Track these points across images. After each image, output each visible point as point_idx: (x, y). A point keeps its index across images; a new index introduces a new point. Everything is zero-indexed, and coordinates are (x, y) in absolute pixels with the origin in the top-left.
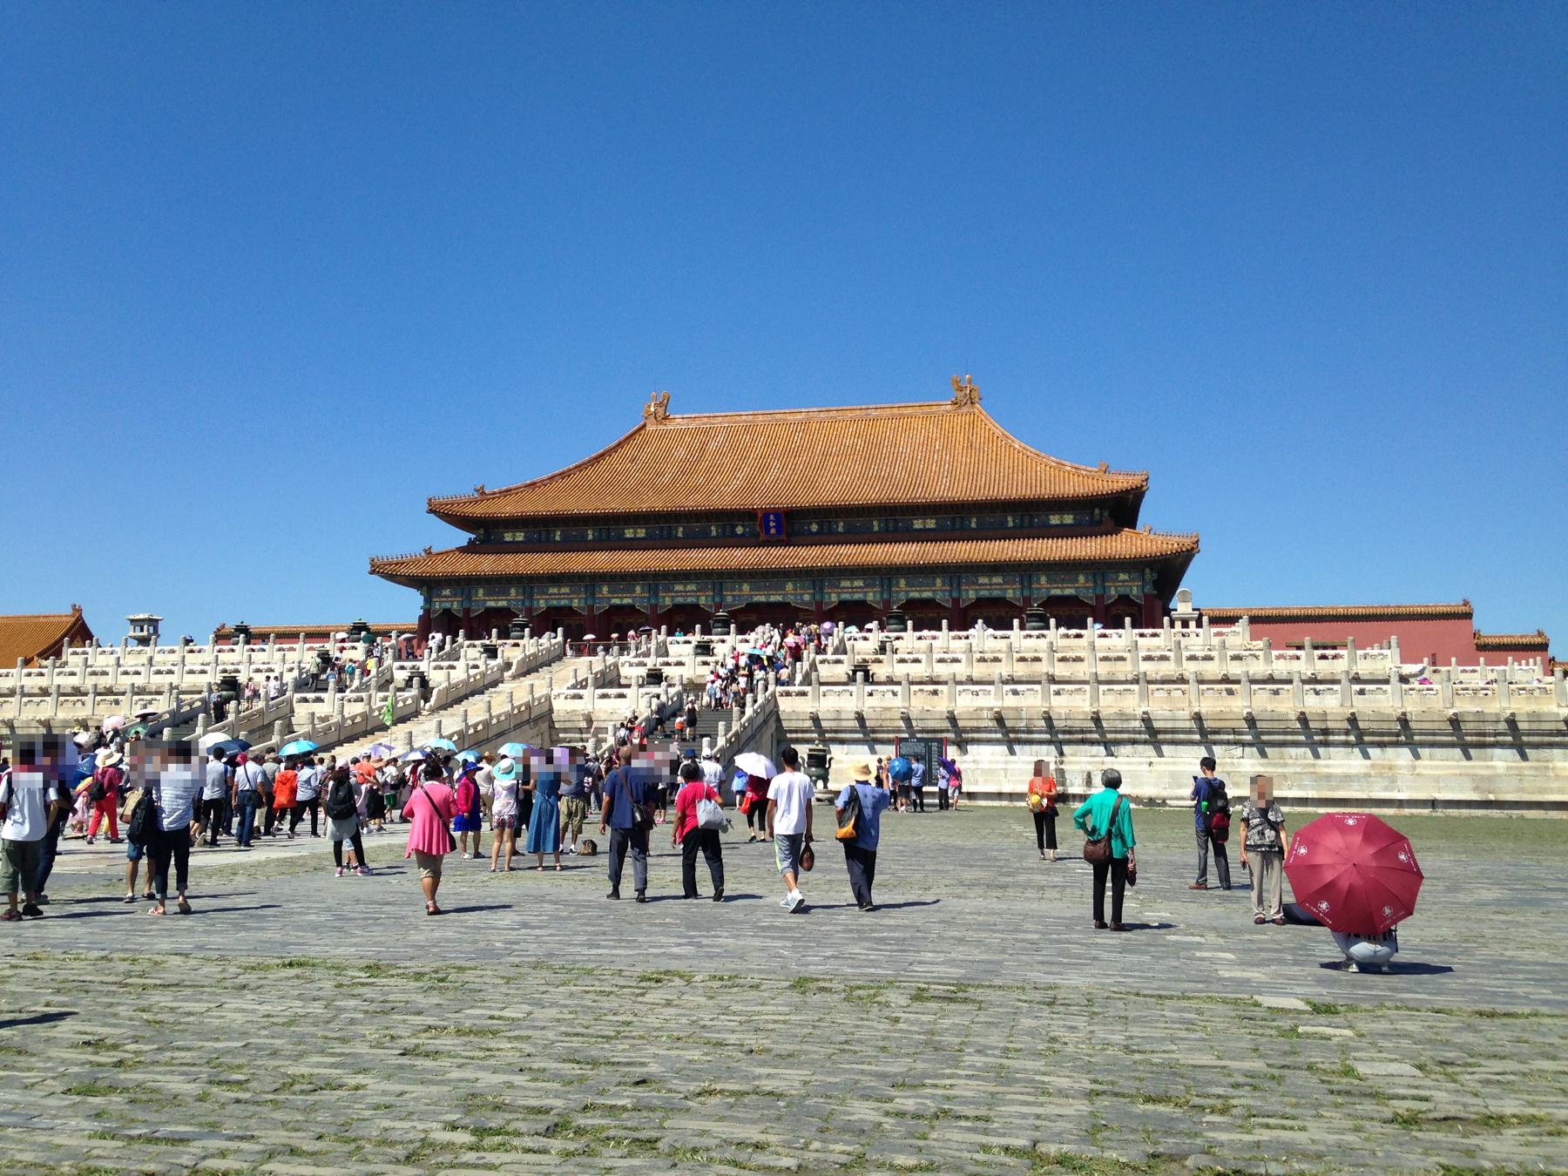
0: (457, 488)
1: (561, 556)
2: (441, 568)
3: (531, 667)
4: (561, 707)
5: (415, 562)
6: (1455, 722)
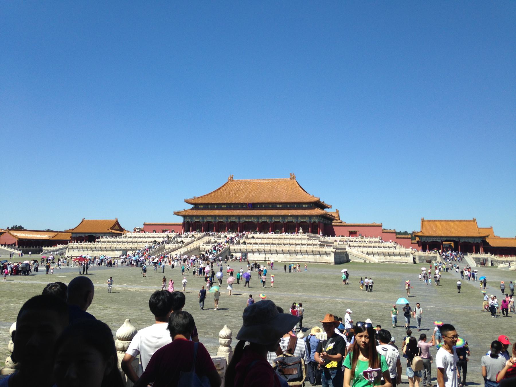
0: (190, 197)
1: (210, 211)
2: (187, 214)
3: (199, 239)
4: (201, 247)
5: (182, 212)
6: (312, 251)
